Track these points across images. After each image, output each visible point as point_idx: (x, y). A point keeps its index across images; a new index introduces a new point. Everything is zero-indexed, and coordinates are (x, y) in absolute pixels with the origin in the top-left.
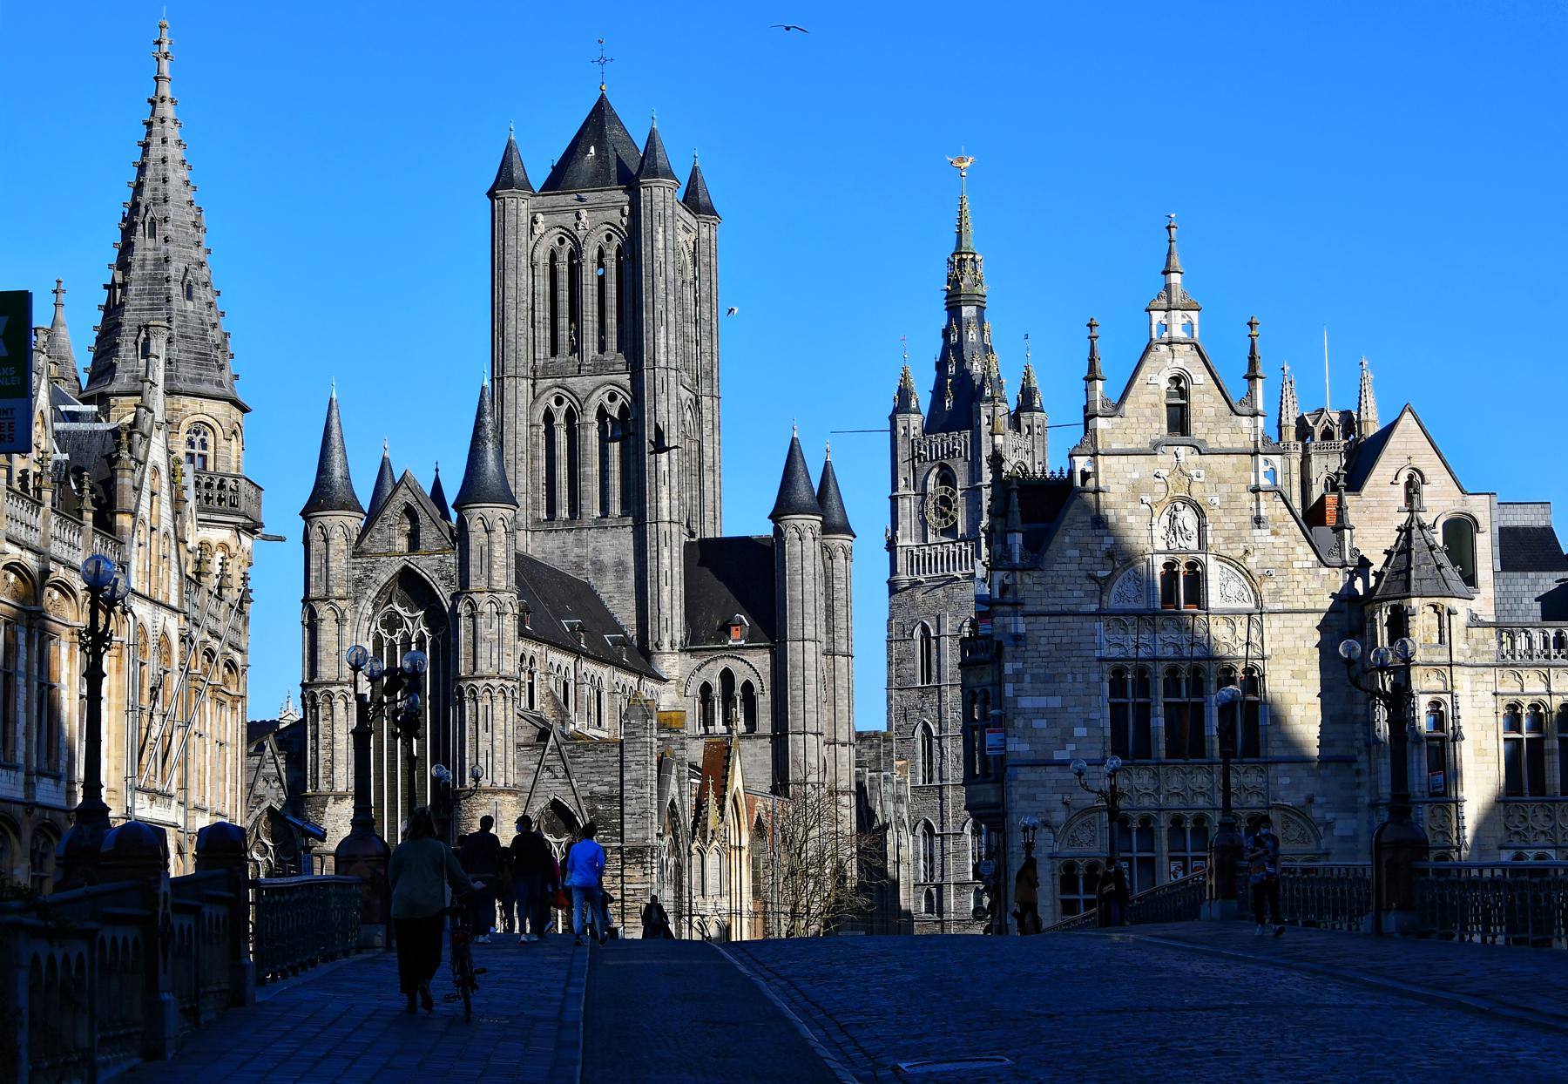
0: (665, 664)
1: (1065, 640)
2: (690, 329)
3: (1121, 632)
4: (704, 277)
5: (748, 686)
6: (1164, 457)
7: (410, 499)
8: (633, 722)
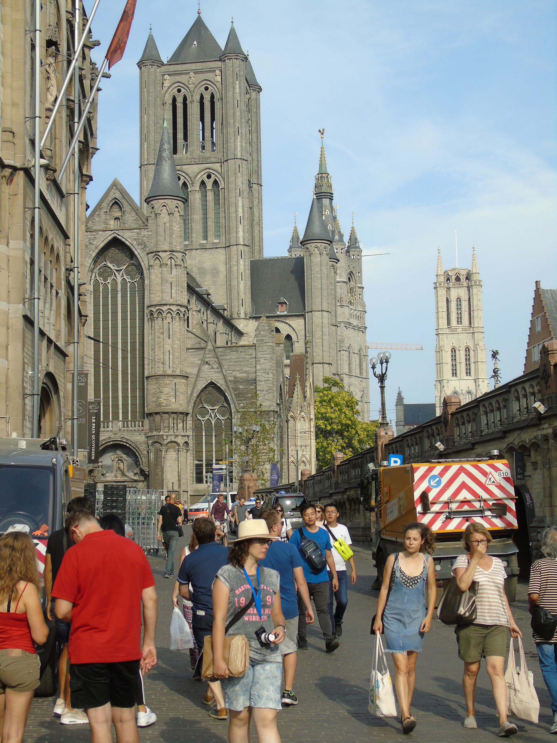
0: (242, 325)
4: (254, 119)
7: (118, 195)
8: (262, 333)
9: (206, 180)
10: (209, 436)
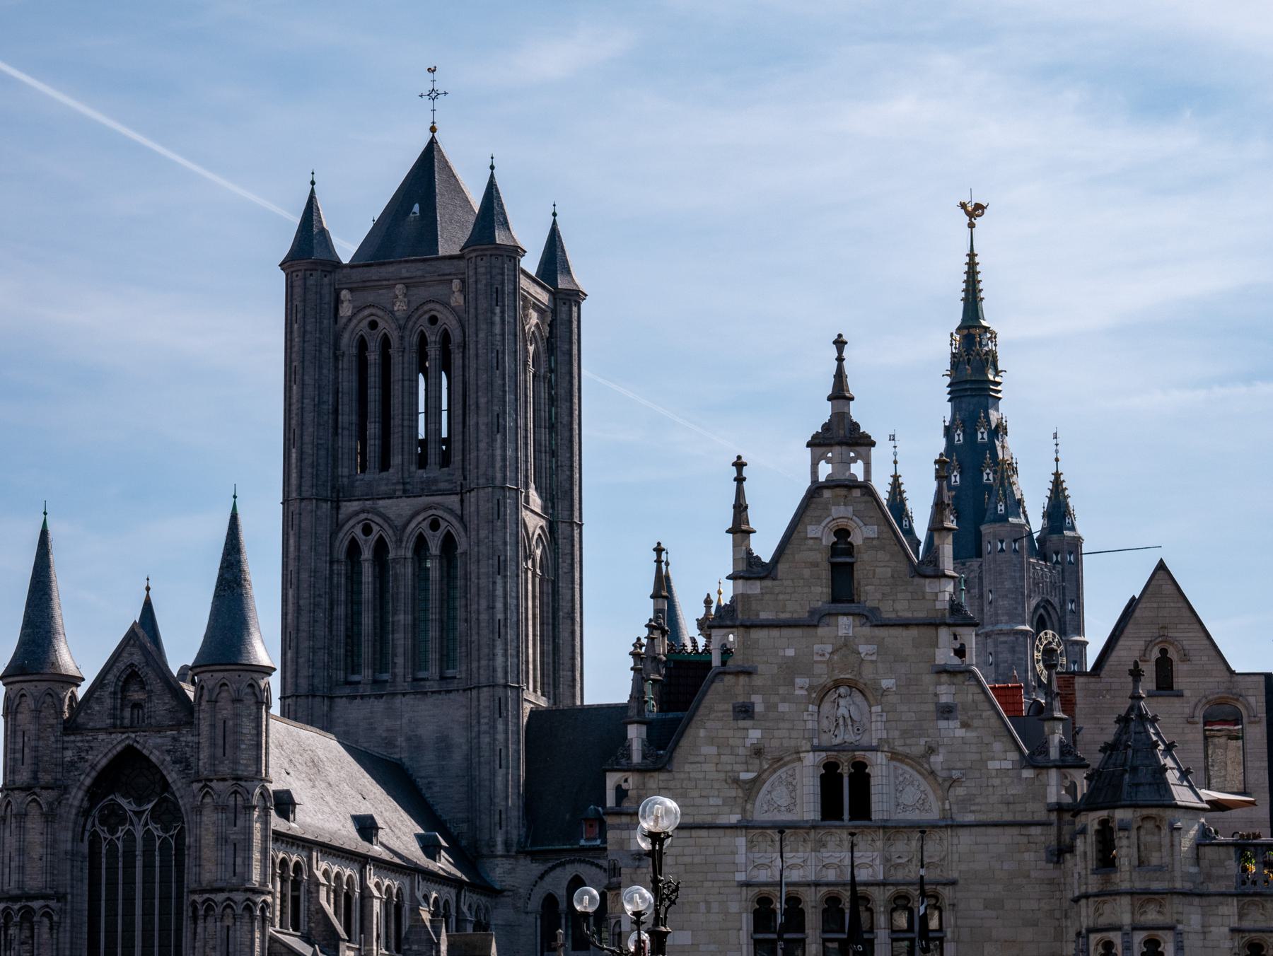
0: (498, 871)
1: (697, 860)
3: (769, 849)
4: (562, 369)
6: (827, 629)
9: (428, 533)
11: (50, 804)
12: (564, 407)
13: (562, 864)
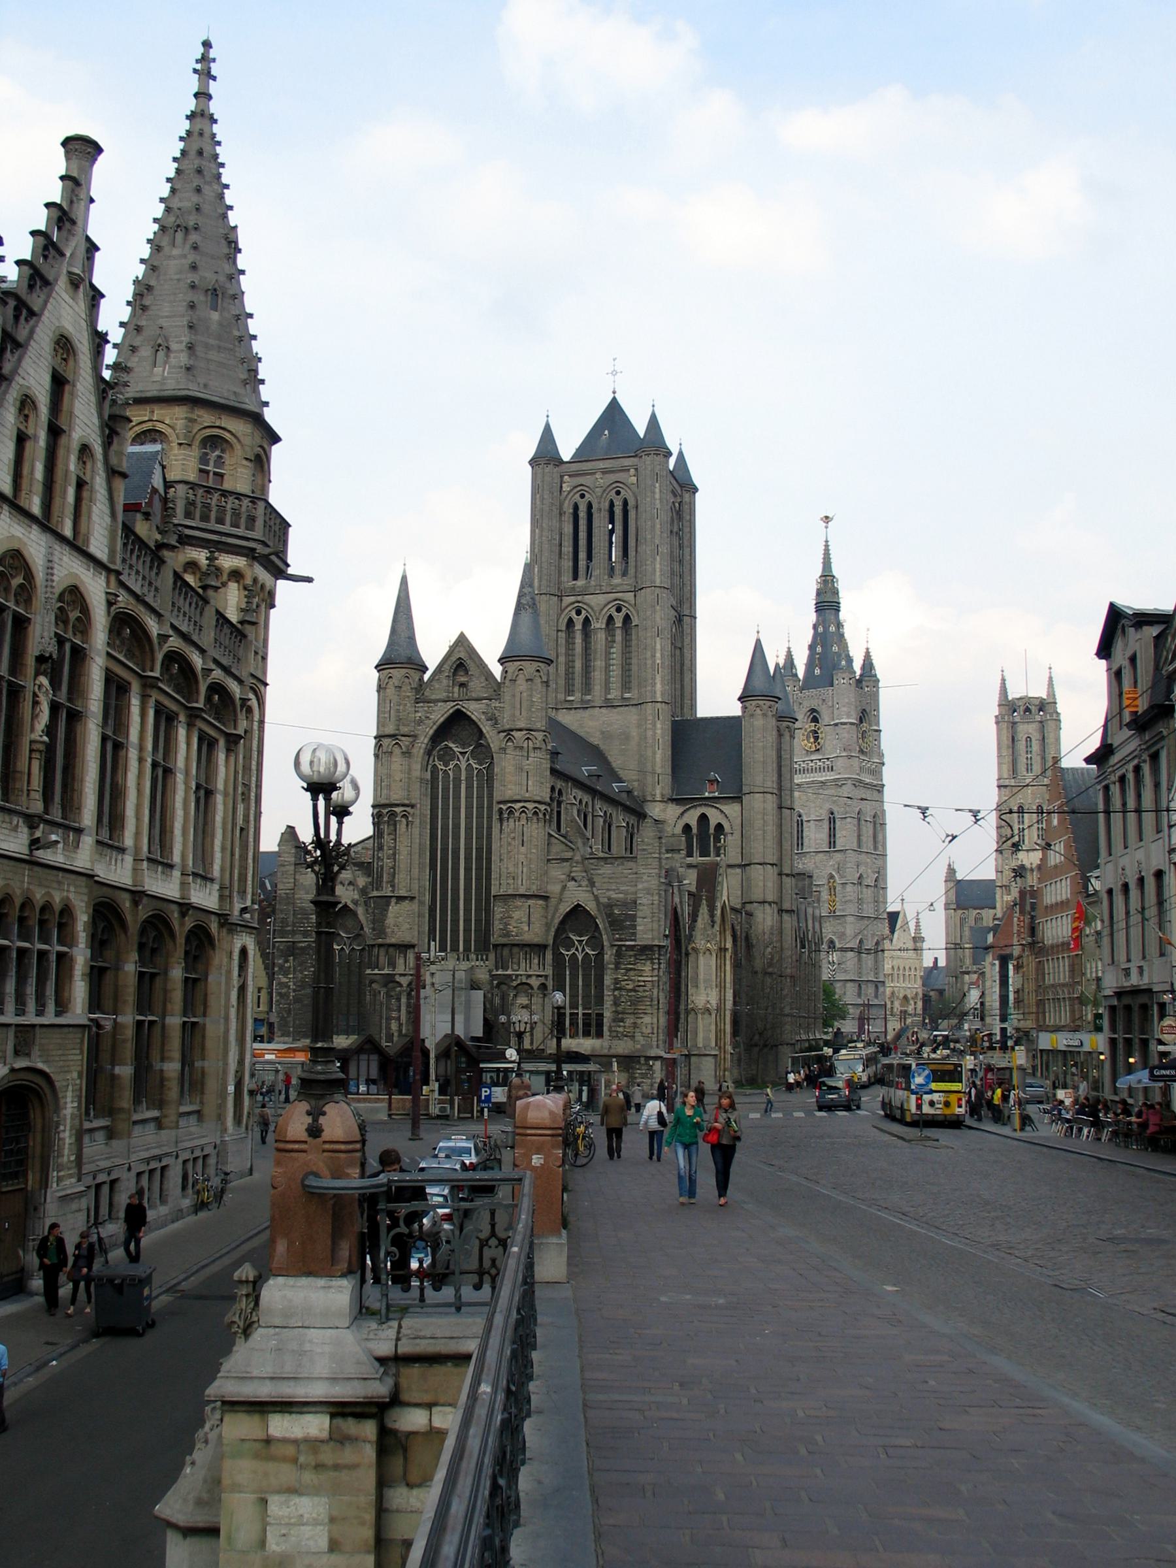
0: (657, 809)
2: (676, 566)
4: (687, 530)
5: (719, 827)
9: (615, 614)
10: (574, 977)
11: (407, 747)
12: (687, 551)
13: (695, 807)
